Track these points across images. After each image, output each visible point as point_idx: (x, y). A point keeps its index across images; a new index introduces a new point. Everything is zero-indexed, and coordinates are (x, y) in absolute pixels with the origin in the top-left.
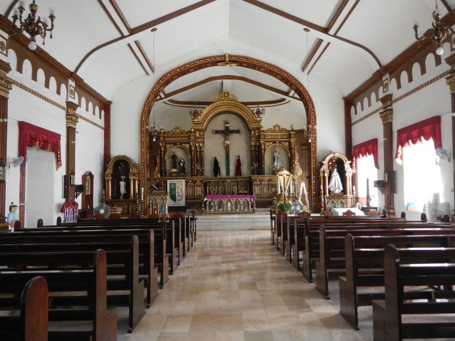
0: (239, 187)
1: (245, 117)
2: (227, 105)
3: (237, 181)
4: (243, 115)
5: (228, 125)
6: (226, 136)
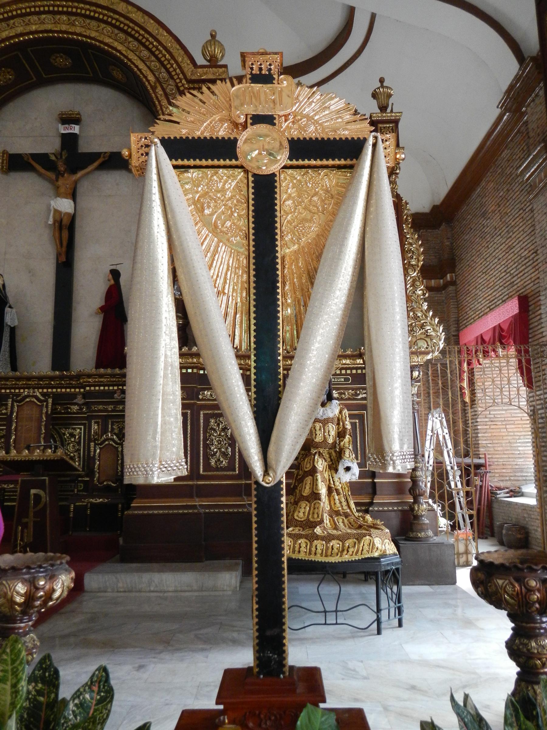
0: (95, 427)
1: (141, 66)
2: (54, 13)
3: (85, 395)
4: (131, 56)
5: (76, 129)
6: (59, 174)
